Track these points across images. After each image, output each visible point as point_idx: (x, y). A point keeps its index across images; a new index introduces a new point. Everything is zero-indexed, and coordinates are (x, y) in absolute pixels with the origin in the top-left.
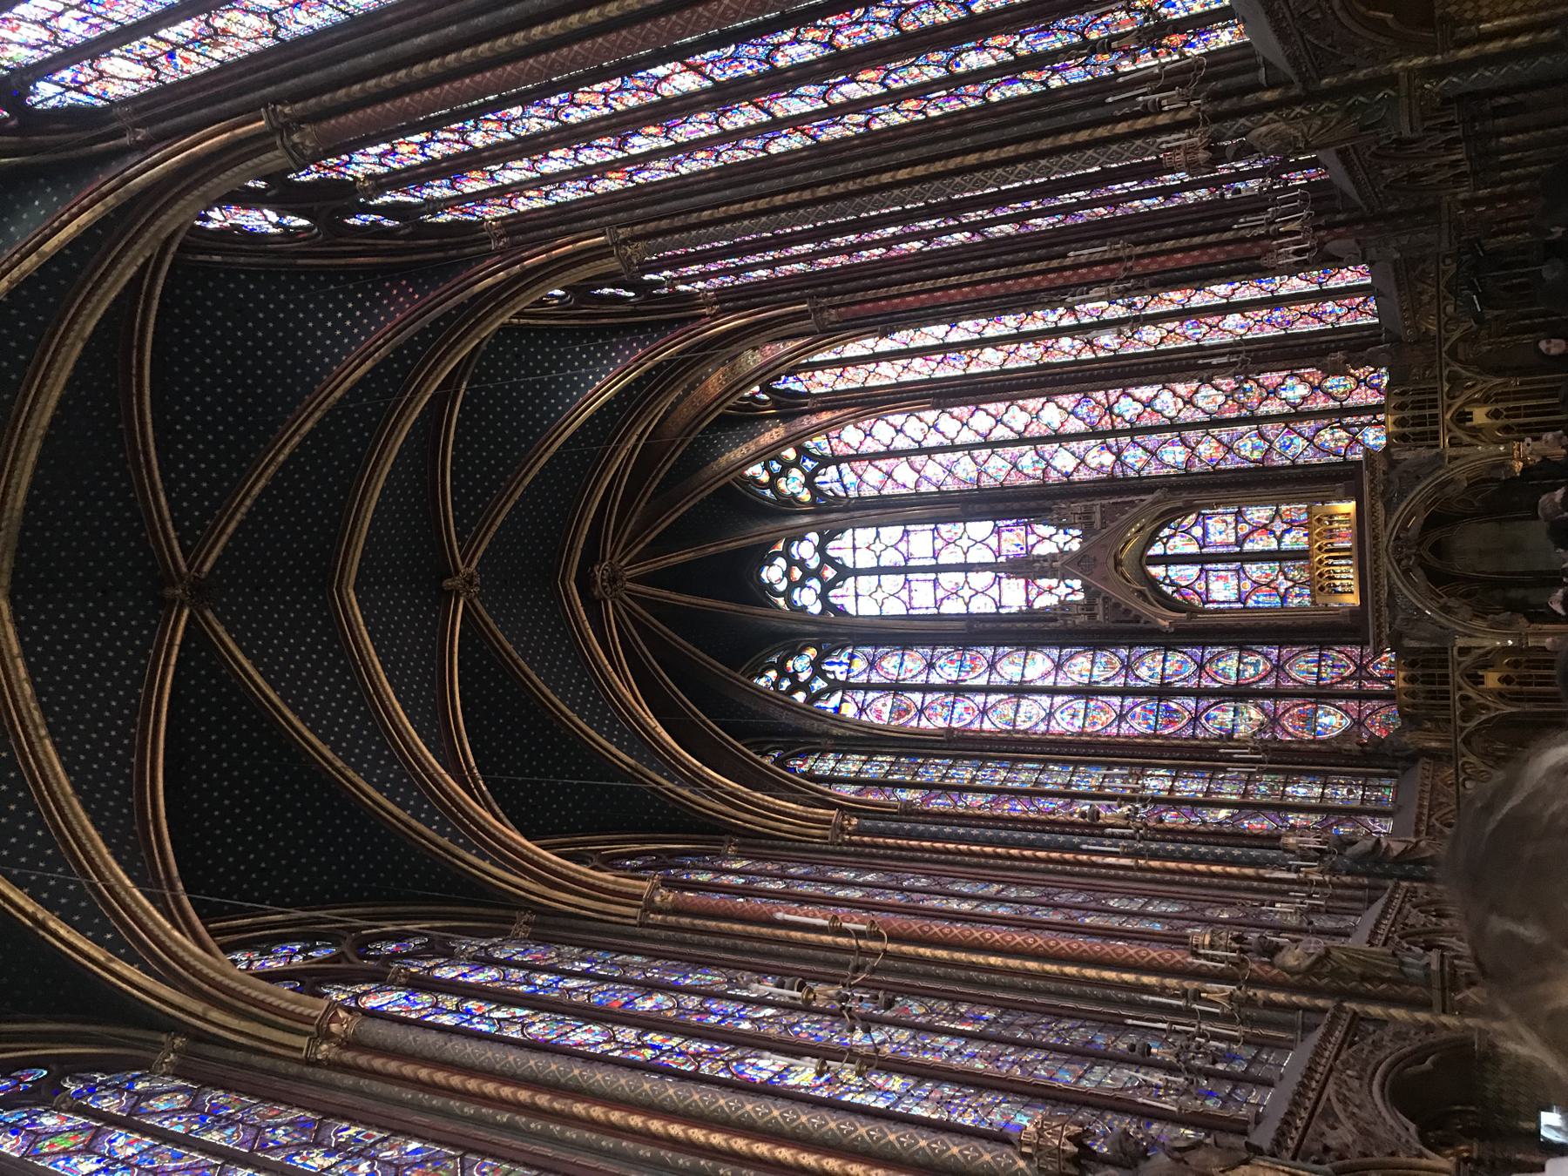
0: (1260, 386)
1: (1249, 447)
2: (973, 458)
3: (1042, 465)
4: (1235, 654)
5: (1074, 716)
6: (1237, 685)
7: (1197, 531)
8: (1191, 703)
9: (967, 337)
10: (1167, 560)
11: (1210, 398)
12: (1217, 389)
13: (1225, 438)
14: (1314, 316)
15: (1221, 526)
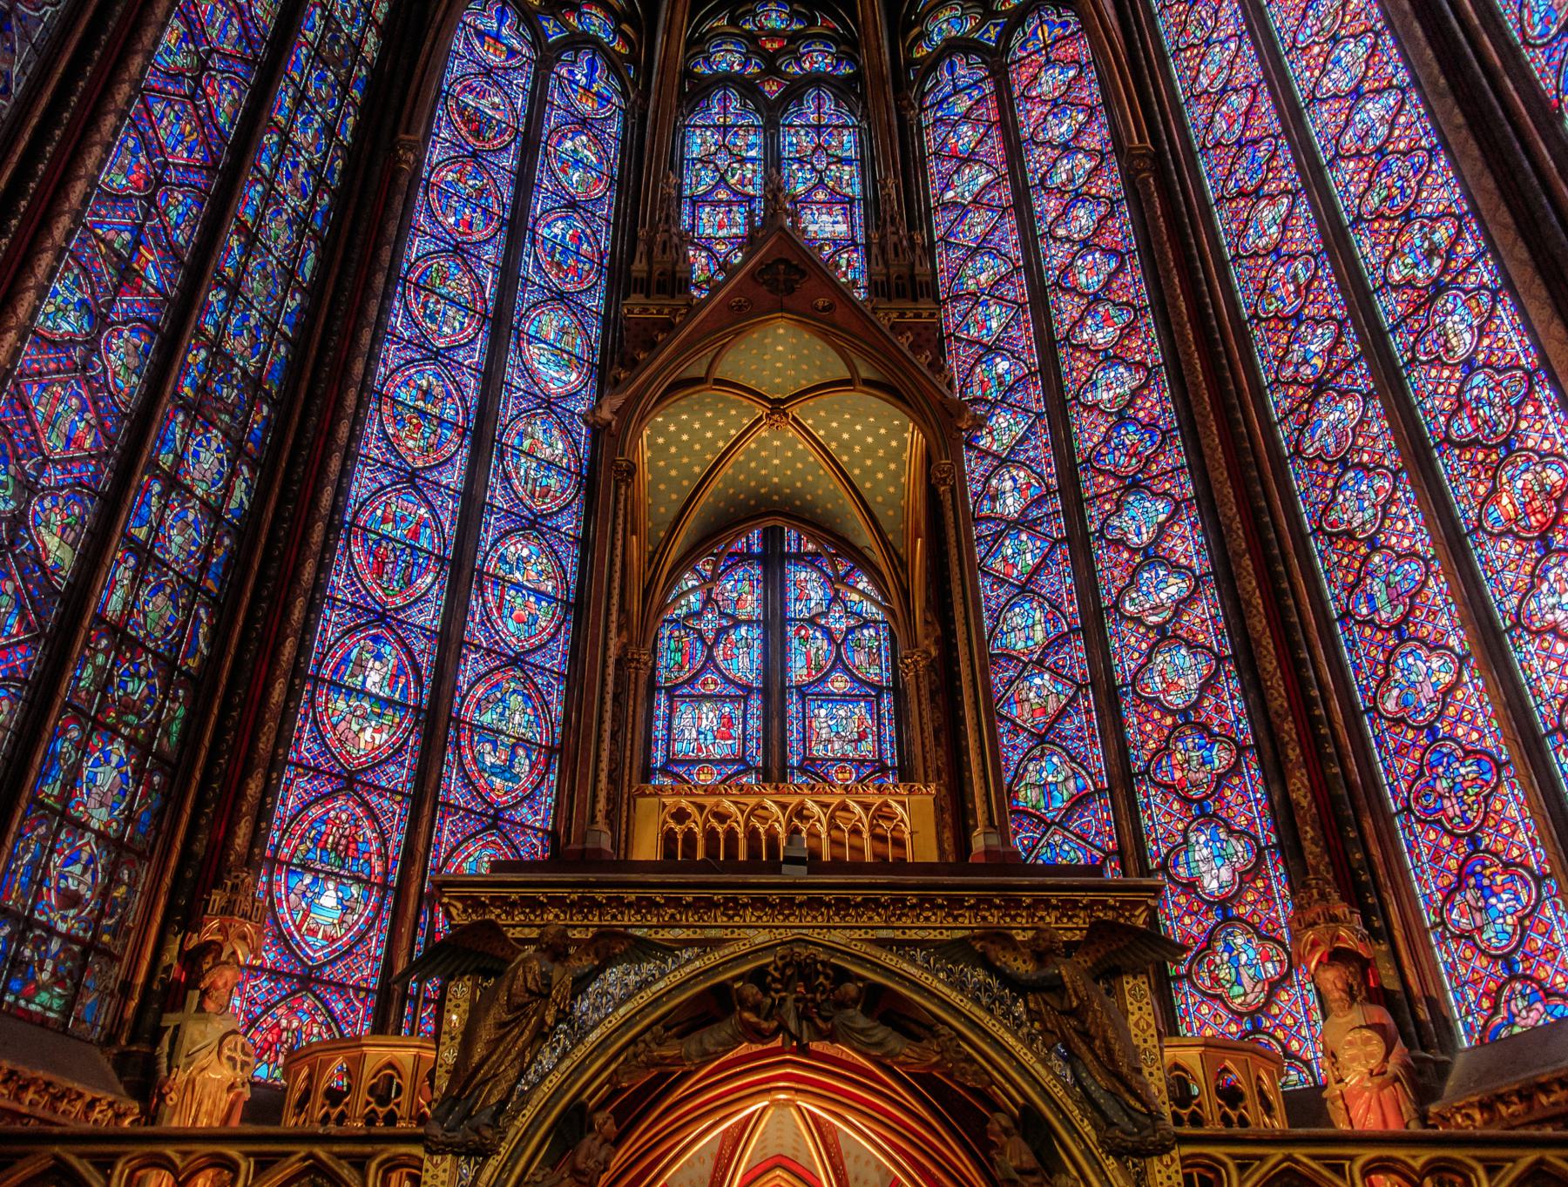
0: (1221, 780)
1: (1049, 780)
2: (1005, 278)
3: (992, 393)
4: (538, 735)
5: (426, 394)
6: (459, 721)
7: (839, 684)
8: (428, 616)
9: (1318, 144)
10: (774, 625)
11: (1179, 674)
12: (1207, 686)
13: (1068, 727)
14: (1463, 875)
15: (853, 729)
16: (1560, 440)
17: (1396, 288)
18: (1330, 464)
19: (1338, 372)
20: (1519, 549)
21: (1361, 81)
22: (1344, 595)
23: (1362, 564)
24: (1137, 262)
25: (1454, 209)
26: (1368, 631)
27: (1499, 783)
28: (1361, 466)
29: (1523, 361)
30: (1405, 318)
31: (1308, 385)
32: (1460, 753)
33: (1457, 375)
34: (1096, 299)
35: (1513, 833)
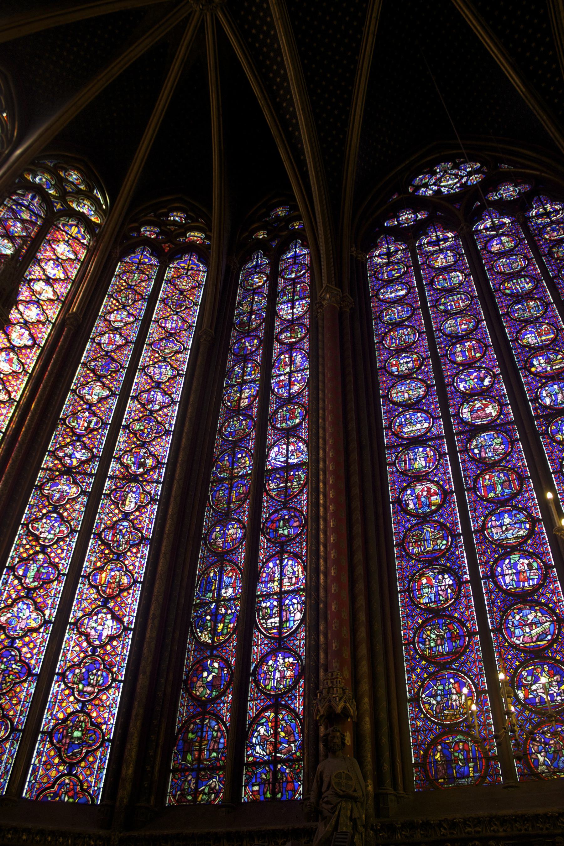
16: (136, 570)
17: (122, 464)
18: (50, 504)
19: (79, 473)
20: (96, 597)
21: (163, 383)
22: (17, 560)
23: (34, 553)
24: (39, 352)
25: (160, 458)
26: (16, 582)
27: (25, 681)
28: (61, 516)
29: (144, 532)
30: (116, 477)
31: (64, 465)
32: (18, 658)
33: (120, 516)
34: (12, 348)
35: (16, 704)
